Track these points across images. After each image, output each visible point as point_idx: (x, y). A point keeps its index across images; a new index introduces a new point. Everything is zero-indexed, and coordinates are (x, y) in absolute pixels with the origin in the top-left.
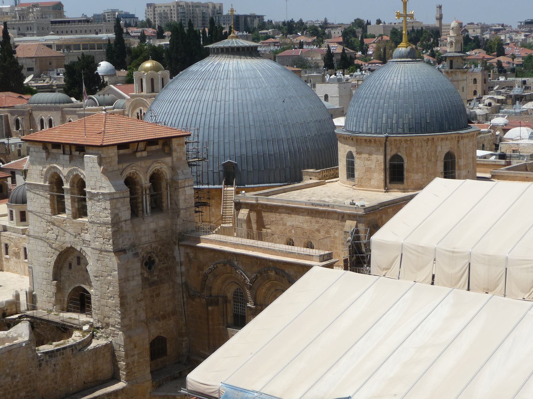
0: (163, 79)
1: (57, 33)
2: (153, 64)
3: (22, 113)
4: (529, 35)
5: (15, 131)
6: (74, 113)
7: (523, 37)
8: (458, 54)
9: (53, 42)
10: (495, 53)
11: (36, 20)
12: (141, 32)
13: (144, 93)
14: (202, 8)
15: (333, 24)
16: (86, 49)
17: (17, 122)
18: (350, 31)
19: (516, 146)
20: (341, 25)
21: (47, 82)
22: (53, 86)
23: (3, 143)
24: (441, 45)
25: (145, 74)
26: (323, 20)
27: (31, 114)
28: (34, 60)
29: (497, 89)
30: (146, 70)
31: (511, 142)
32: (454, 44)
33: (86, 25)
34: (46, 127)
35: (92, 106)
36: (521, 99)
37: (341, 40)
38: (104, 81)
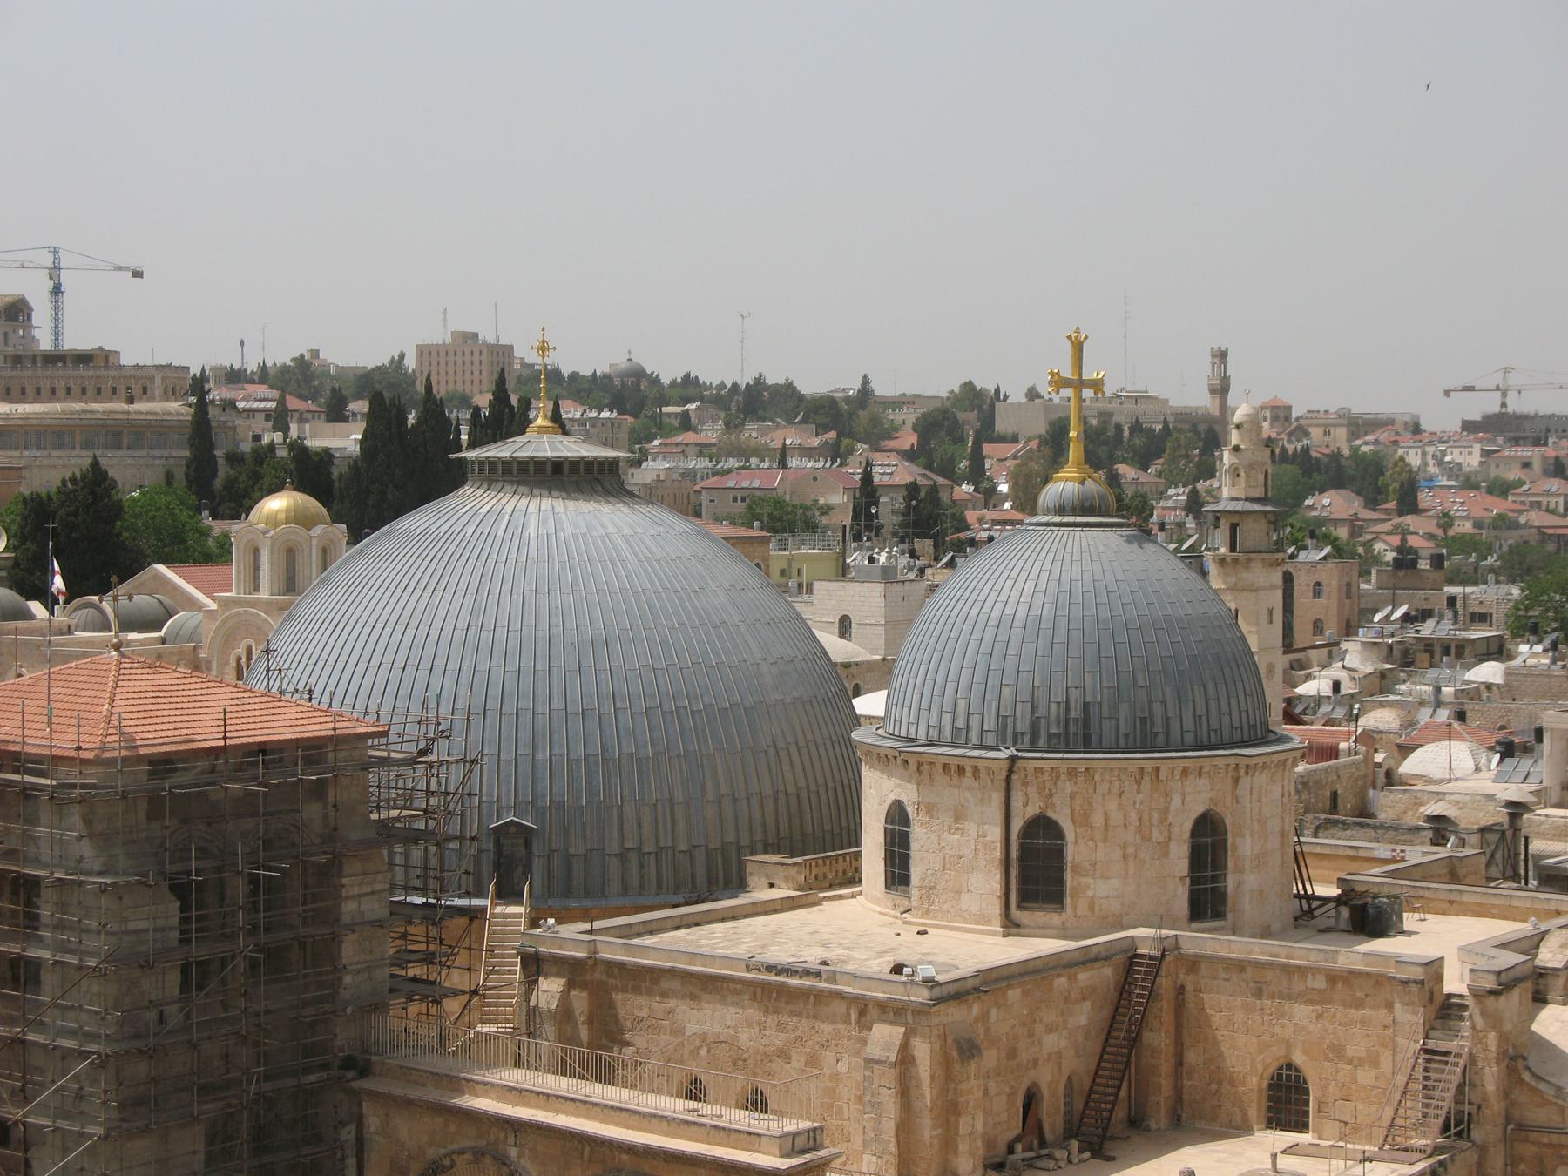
0: (324, 551)
4: (1498, 451)
8: (1257, 507)
13: (264, 594)
26: (857, 385)
30: (272, 520)
32: (1242, 474)
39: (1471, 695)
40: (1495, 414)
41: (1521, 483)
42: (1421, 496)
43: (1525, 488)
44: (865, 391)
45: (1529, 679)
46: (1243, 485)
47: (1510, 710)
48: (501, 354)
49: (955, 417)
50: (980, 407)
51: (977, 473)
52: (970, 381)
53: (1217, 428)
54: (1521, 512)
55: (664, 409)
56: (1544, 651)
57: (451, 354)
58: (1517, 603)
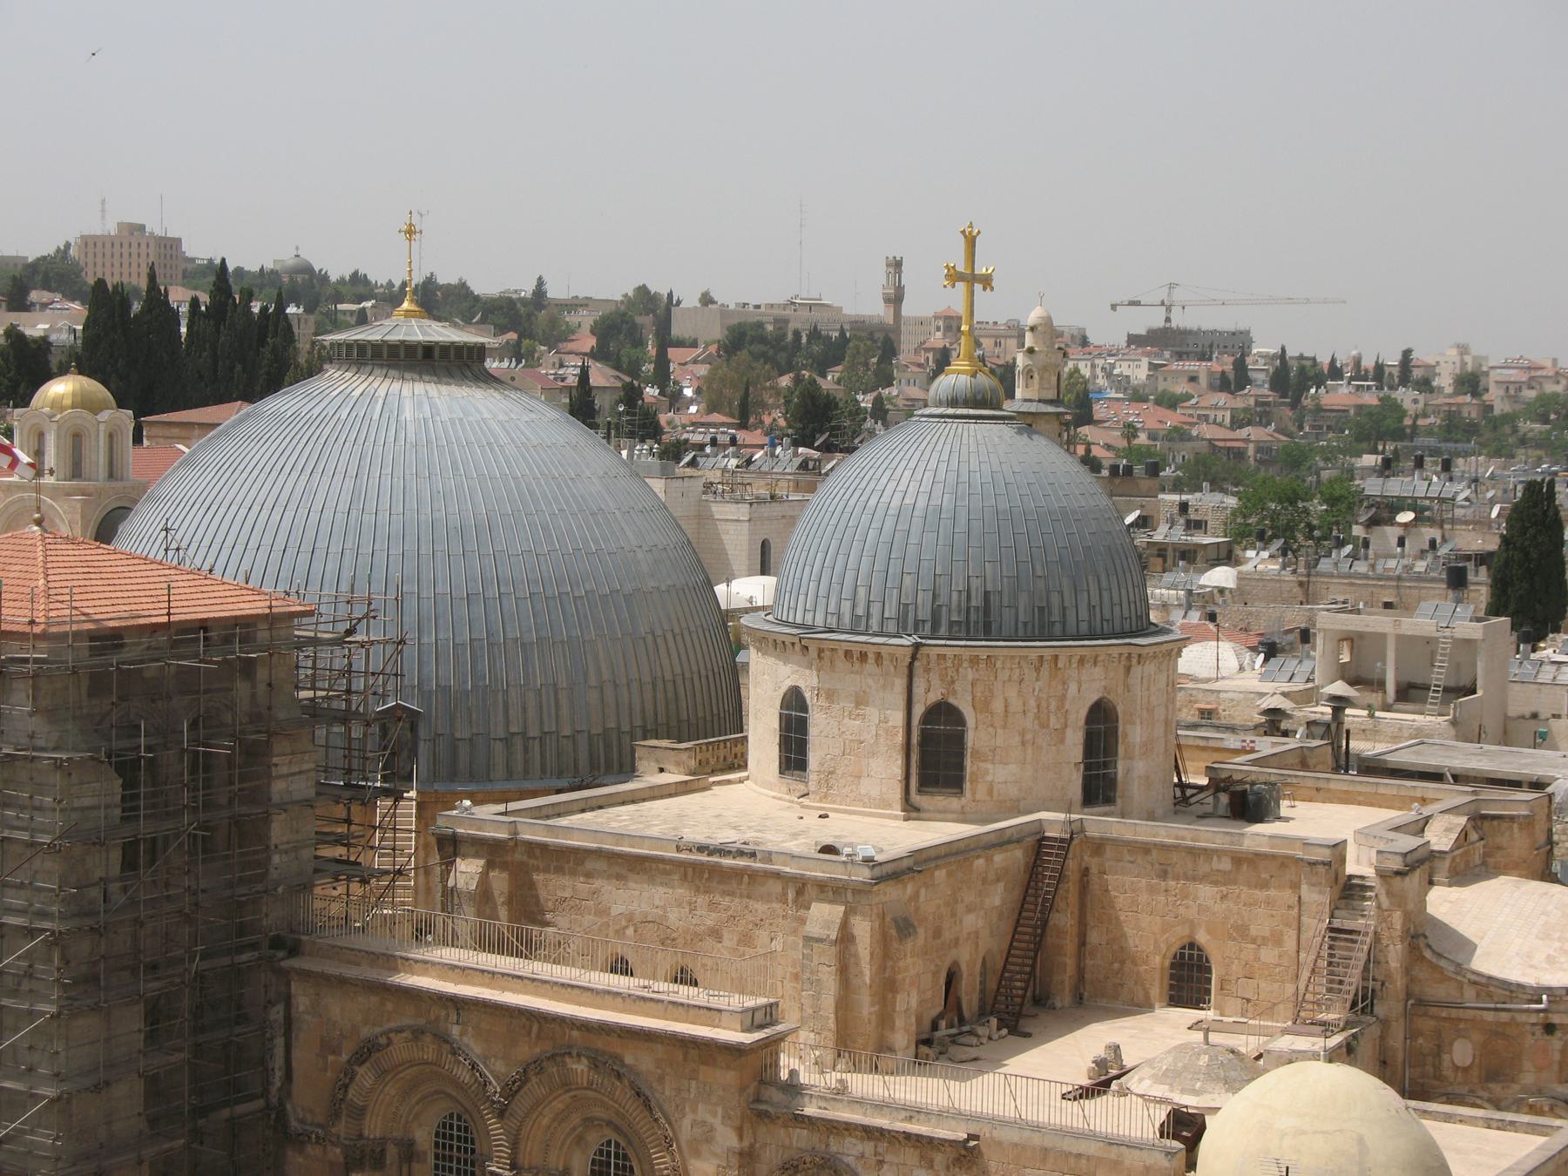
0: (111, 436)
4: (1165, 365)
8: (1050, 409)
20: (586, 302)
30: (57, 405)
31: (1191, 685)
32: (1036, 376)
39: (1206, 598)
40: (1159, 329)
41: (1189, 397)
42: (1096, 407)
43: (1193, 401)
44: (540, 292)
45: (1260, 584)
46: (1036, 387)
47: (1251, 613)
48: (168, 247)
49: (633, 321)
50: (653, 312)
51: (662, 376)
52: (644, 286)
53: (892, 336)
54: (1192, 424)
55: (339, 306)
56: (1270, 557)
57: (117, 245)
58: (1234, 513)
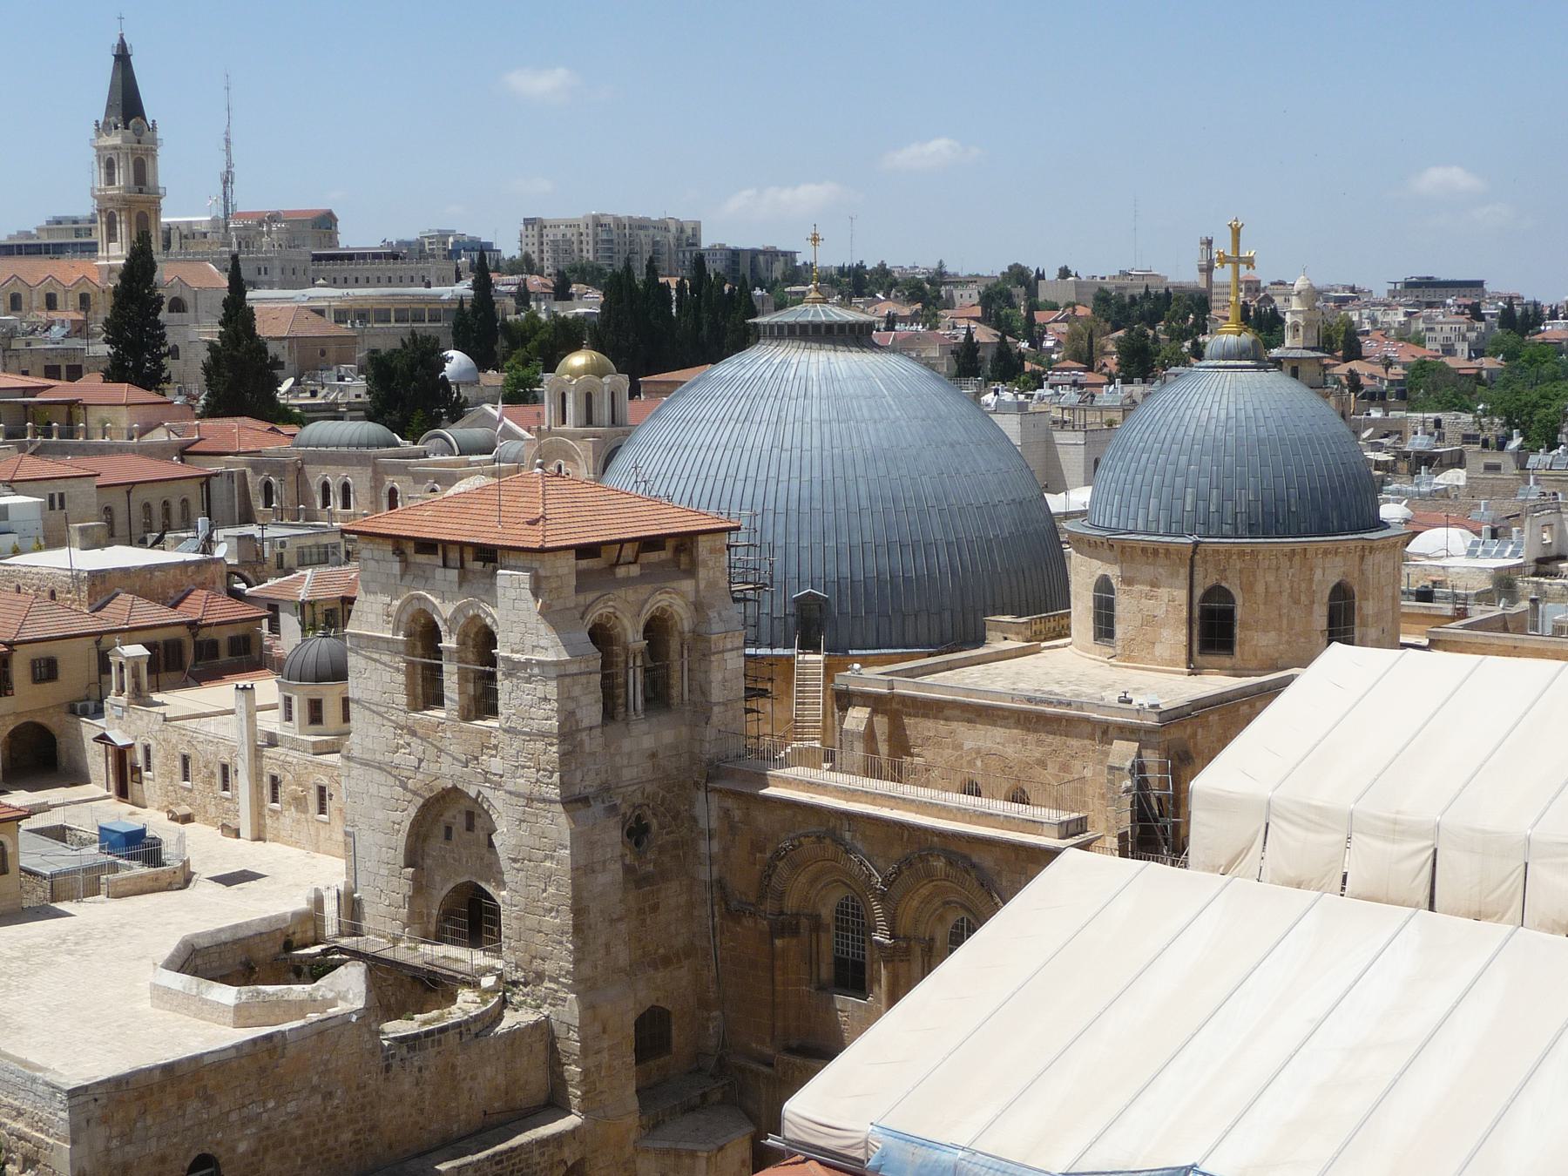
0: (613, 394)
1: (334, 283)
2: (592, 358)
3: (279, 468)
4: (1415, 313)
5: (261, 508)
6: (403, 470)
7: (1402, 319)
9: (327, 304)
10: (1340, 353)
11: (279, 253)
12: (519, 284)
13: (569, 426)
14: (651, 232)
15: (956, 275)
16: (402, 321)
17: (268, 487)
18: (1000, 293)
19: (1441, 572)
21: (325, 397)
22: (338, 405)
23: (252, 537)
24: (1211, 332)
25: (574, 382)
26: (936, 266)
27: (300, 471)
28: (286, 343)
29: (1369, 438)
30: (575, 373)
31: (1427, 562)
32: (1301, 329)
33: (391, 264)
34: (336, 505)
35: (442, 455)
36: (1427, 461)
37: (978, 311)
38: (459, 396)
46: (1301, 338)
